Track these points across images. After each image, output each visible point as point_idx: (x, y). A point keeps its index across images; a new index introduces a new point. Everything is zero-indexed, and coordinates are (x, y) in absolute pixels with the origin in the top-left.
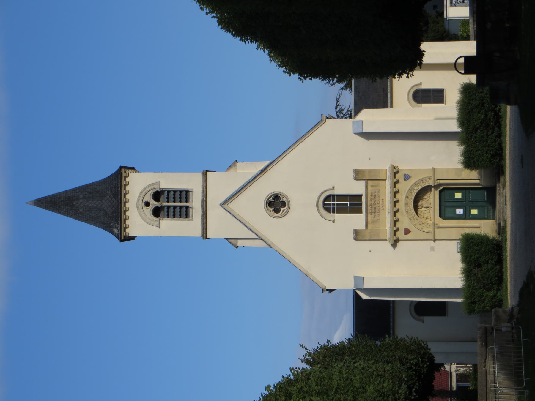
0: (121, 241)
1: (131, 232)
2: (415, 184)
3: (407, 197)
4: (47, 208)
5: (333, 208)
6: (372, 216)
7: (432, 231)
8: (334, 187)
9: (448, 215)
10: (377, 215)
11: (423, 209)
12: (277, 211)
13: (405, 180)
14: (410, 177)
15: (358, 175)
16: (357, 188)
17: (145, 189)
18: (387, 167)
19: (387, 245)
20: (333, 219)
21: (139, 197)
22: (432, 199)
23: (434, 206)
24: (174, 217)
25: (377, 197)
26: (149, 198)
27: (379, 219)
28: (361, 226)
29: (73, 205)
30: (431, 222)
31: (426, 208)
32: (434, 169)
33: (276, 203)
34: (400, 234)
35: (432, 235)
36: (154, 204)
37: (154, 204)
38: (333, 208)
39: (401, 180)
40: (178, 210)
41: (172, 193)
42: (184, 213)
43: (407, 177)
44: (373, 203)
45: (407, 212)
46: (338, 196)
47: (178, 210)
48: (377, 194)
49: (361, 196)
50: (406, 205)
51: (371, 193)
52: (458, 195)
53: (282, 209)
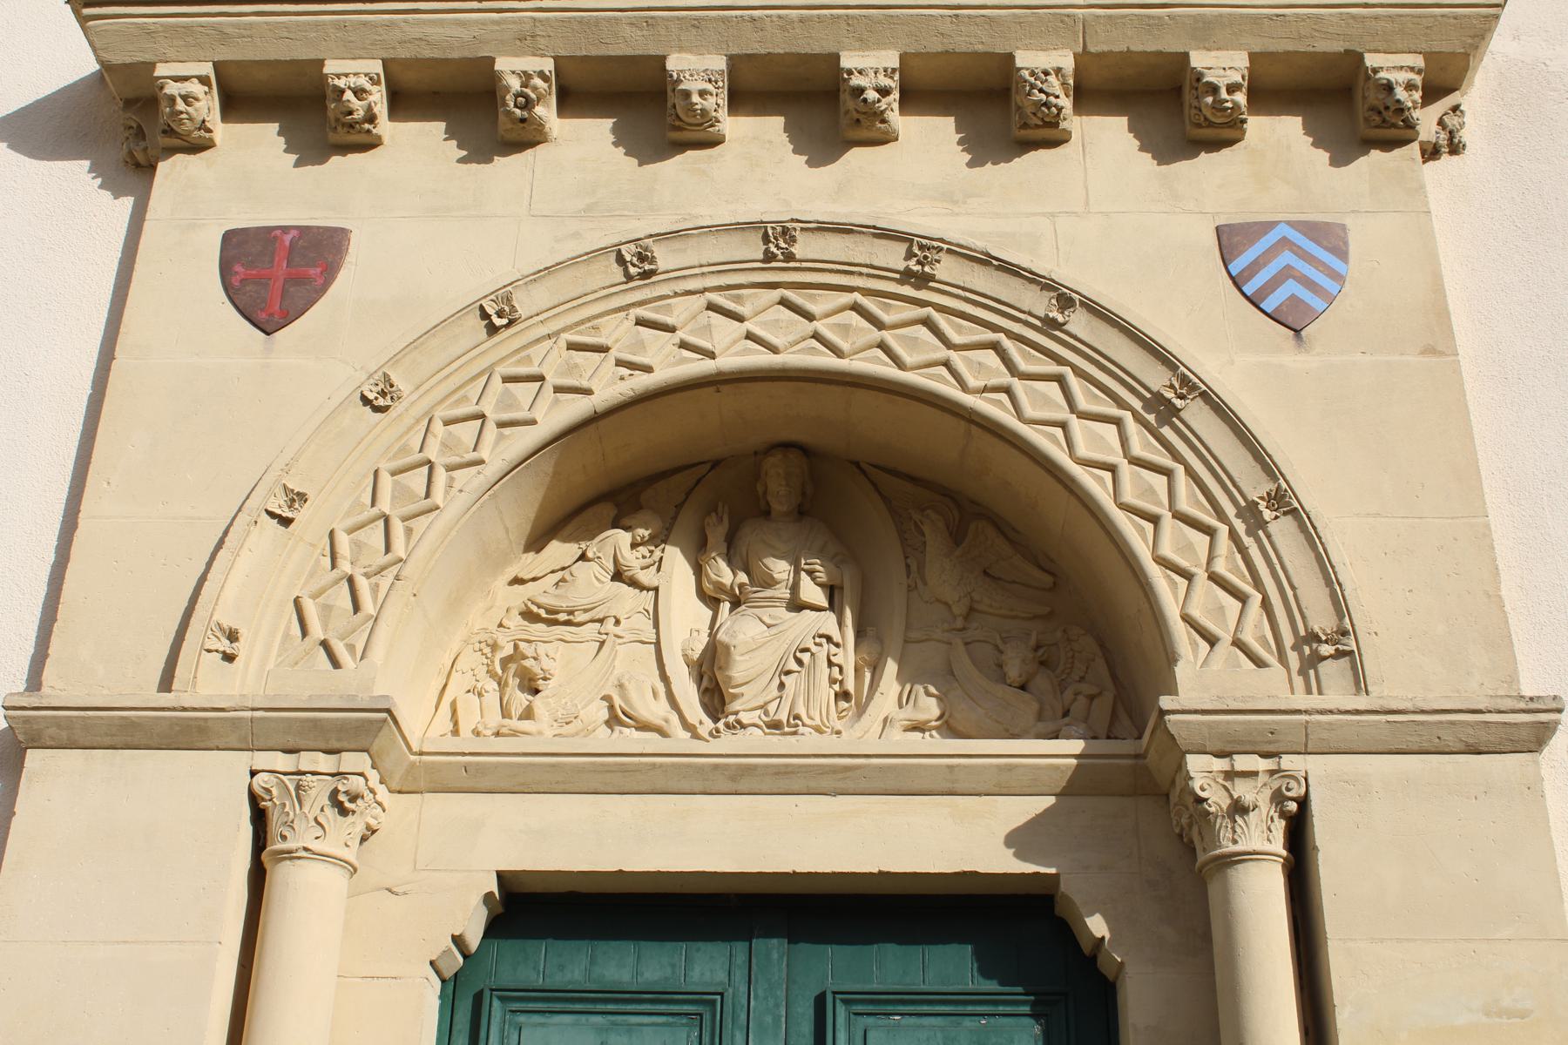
2: (1170, 399)
3: (920, 261)
7: (208, 685)
11: (687, 621)
13: (1229, 240)
23: (739, 779)
31: (712, 677)
34: (248, 174)
35: (130, 684)
43: (1274, 277)
45: (637, 264)
50: (777, 240)
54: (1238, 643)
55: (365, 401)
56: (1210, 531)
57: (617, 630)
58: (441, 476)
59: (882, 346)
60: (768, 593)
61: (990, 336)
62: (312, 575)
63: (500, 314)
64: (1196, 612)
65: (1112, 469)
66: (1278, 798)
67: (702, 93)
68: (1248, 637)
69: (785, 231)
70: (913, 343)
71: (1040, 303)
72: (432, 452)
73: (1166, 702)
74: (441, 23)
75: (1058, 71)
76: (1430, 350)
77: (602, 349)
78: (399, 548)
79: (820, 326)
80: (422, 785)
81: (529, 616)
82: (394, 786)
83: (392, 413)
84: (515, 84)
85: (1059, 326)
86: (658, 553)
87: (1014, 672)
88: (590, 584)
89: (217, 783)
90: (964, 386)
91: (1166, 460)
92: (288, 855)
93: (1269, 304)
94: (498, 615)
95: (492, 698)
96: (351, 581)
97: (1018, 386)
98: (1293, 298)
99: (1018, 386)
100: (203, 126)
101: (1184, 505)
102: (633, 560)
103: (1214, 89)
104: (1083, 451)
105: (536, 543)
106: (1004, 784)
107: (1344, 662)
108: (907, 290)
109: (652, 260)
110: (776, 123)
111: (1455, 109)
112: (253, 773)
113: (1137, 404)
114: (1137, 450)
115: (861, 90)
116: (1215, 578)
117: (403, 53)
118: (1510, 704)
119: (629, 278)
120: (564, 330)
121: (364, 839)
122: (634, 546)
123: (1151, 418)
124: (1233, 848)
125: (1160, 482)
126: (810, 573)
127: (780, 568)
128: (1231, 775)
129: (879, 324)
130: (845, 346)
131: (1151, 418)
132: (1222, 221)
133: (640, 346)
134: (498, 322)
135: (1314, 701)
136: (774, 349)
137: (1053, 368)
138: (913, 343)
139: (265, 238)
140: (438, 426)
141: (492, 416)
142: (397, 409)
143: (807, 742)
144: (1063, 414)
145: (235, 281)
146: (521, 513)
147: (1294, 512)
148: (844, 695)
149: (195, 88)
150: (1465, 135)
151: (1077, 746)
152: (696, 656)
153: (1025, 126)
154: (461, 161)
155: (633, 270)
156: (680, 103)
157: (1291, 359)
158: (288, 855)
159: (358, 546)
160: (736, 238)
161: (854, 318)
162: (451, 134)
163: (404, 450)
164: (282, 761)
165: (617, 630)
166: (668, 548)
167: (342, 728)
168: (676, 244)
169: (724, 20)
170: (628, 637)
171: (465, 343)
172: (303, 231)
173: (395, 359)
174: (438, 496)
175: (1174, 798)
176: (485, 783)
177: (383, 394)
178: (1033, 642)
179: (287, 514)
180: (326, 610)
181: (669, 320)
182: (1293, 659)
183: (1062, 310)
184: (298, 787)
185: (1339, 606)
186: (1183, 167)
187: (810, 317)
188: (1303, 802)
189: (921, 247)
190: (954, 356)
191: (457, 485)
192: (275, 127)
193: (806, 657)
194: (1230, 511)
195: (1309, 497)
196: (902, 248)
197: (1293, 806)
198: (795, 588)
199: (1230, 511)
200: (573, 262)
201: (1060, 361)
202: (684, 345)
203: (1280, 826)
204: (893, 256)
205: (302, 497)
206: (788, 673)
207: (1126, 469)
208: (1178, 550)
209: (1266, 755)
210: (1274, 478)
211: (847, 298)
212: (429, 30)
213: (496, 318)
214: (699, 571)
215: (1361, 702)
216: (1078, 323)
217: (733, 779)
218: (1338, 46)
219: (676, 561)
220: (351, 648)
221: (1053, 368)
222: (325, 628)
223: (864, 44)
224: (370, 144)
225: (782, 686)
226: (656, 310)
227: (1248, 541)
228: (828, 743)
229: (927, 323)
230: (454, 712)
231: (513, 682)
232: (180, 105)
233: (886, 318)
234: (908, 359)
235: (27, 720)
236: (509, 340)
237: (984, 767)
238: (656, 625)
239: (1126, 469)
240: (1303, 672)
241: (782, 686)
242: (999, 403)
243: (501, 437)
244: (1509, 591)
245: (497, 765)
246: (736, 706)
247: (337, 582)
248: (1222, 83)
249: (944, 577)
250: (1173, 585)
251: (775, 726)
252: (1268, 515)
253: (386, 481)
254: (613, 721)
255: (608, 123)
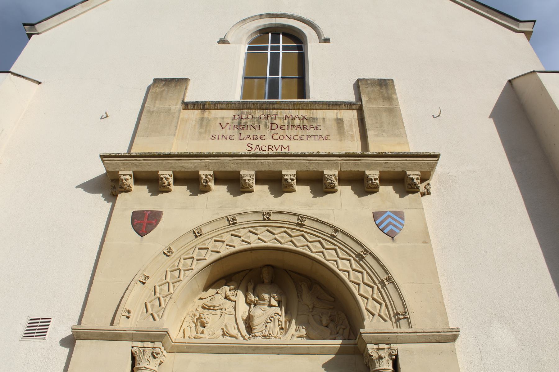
2: (362, 255)
3: (301, 221)
6: (230, 121)
7: (122, 324)
8: (327, 40)
10: (228, 132)
11: (243, 309)
13: (376, 215)
14: (391, 235)
20: (229, 39)
25: (300, 132)
27: (214, 137)
31: (249, 323)
32: (452, 337)
34: (139, 198)
35: (103, 324)
39: (373, 202)
43: (387, 224)
44: (277, 121)
45: (232, 221)
48: (312, 132)
50: (266, 215)
51: (314, 119)
54: (379, 315)
55: (165, 253)
56: (372, 287)
57: (225, 312)
58: (182, 272)
59: (292, 241)
60: (263, 302)
61: (318, 239)
62: (149, 297)
63: (198, 233)
64: (369, 308)
65: (348, 272)
66: (390, 355)
67: (249, 180)
68: (382, 314)
69: (268, 213)
70: (299, 241)
71: (330, 231)
72: (180, 267)
73: (362, 331)
74: (187, 163)
75: (334, 175)
76: (425, 242)
77: (223, 242)
78: (171, 290)
79: (276, 236)
80: (175, 351)
81: (203, 308)
82: (168, 351)
83: (171, 257)
84: (204, 177)
85: (335, 237)
86: (236, 292)
87: (324, 322)
88: (219, 300)
89: (124, 349)
90: (312, 252)
91: (361, 270)
92: (140, 369)
93: (386, 231)
94: (196, 307)
95: (194, 328)
96: (159, 298)
97: (325, 251)
98: (392, 230)
99: (325, 251)
100: (129, 186)
101: (366, 281)
102: (230, 294)
103: (371, 180)
104: (341, 267)
105: (206, 289)
106: (322, 351)
107: (406, 320)
108: (298, 228)
109: (236, 220)
110: (266, 187)
111: (428, 184)
112: (132, 347)
113: (354, 256)
114: (354, 267)
115: (287, 179)
116: (374, 299)
117: (177, 170)
118: (447, 330)
119: (230, 224)
120: (214, 237)
121: (160, 365)
122: (230, 290)
123: (357, 259)
124: (379, 368)
125: (360, 275)
126: (274, 297)
127: (266, 296)
128: (378, 349)
129: (291, 236)
130: (282, 241)
131: (357, 259)
132: (374, 211)
133: (232, 241)
134: (198, 234)
135: (399, 330)
136: (265, 242)
137: (333, 247)
138: (299, 241)
139: (143, 213)
140: (182, 260)
141: (195, 258)
142: (172, 256)
143: (272, 341)
144: (336, 258)
145: (135, 224)
146: (202, 282)
147: (393, 282)
148: (282, 329)
149: (128, 177)
150: (431, 190)
151: (340, 342)
152: (245, 318)
153: (326, 188)
154: (190, 195)
155: (231, 222)
156: (243, 182)
157: (391, 244)
158: (140, 369)
159: (161, 290)
160: (256, 215)
161: (285, 234)
162: (188, 189)
163: (174, 266)
164: (140, 344)
165: (225, 312)
166: (239, 291)
167: (155, 336)
168: (242, 216)
169: (254, 162)
170: (228, 313)
171: (189, 240)
172: (152, 211)
173: (172, 243)
174: (181, 278)
175: (364, 355)
176: (191, 351)
177: (169, 252)
178: (329, 315)
179: (144, 281)
180: (153, 306)
181: (240, 235)
182: (393, 319)
183: (335, 233)
184: (144, 351)
185: (404, 306)
186: (364, 198)
187: (274, 234)
188: (397, 356)
189: (301, 217)
190: (309, 244)
191: (186, 275)
192: (146, 186)
193: (272, 319)
194: (377, 282)
195: (397, 278)
196: (297, 217)
197: (394, 357)
198: (270, 301)
199: (377, 282)
200: (216, 220)
201: (335, 245)
202: (243, 241)
203: (391, 362)
204: (294, 219)
205: (148, 277)
206: (268, 323)
207: (351, 272)
208: (365, 292)
209: (387, 344)
210: (388, 274)
211: (283, 230)
212: (184, 164)
213: (197, 234)
214: (246, 297)
215: (410, 330)
216: (340, 236)
217: (253, 350)
218: (400, 170)
219: (240, 294)
220: (158, 316)
221: (333, 247)
222: (152, 310)
223: (288, 169)
224: (169, 191)
225: (266, 326)
226: (236, 232)
227: (382, 290)
228: (278, 341)
229: (303, 236)
230: (184, 332)
231: (199, 324)
232: (124, 181)
233: (293, 234)
234: (298, 245)
235: (77, 332)
236: (200, 239)
237: (317, 347)
238: (235, 310)
239: (351, 272)
240: (396, 323)
241: (266, 326)
242: (320, 256)
243: (197, 263)
244: (445, 301)
245: (194, 346)
246: (255, 331)
247: (156, 298)
248: (373, 178)
249: (307, 299)
250: (363, 301)
251: (264, 336)
252: (386, 283)
253: (169, 273)
254: (224, 335)
255: (226, 187)
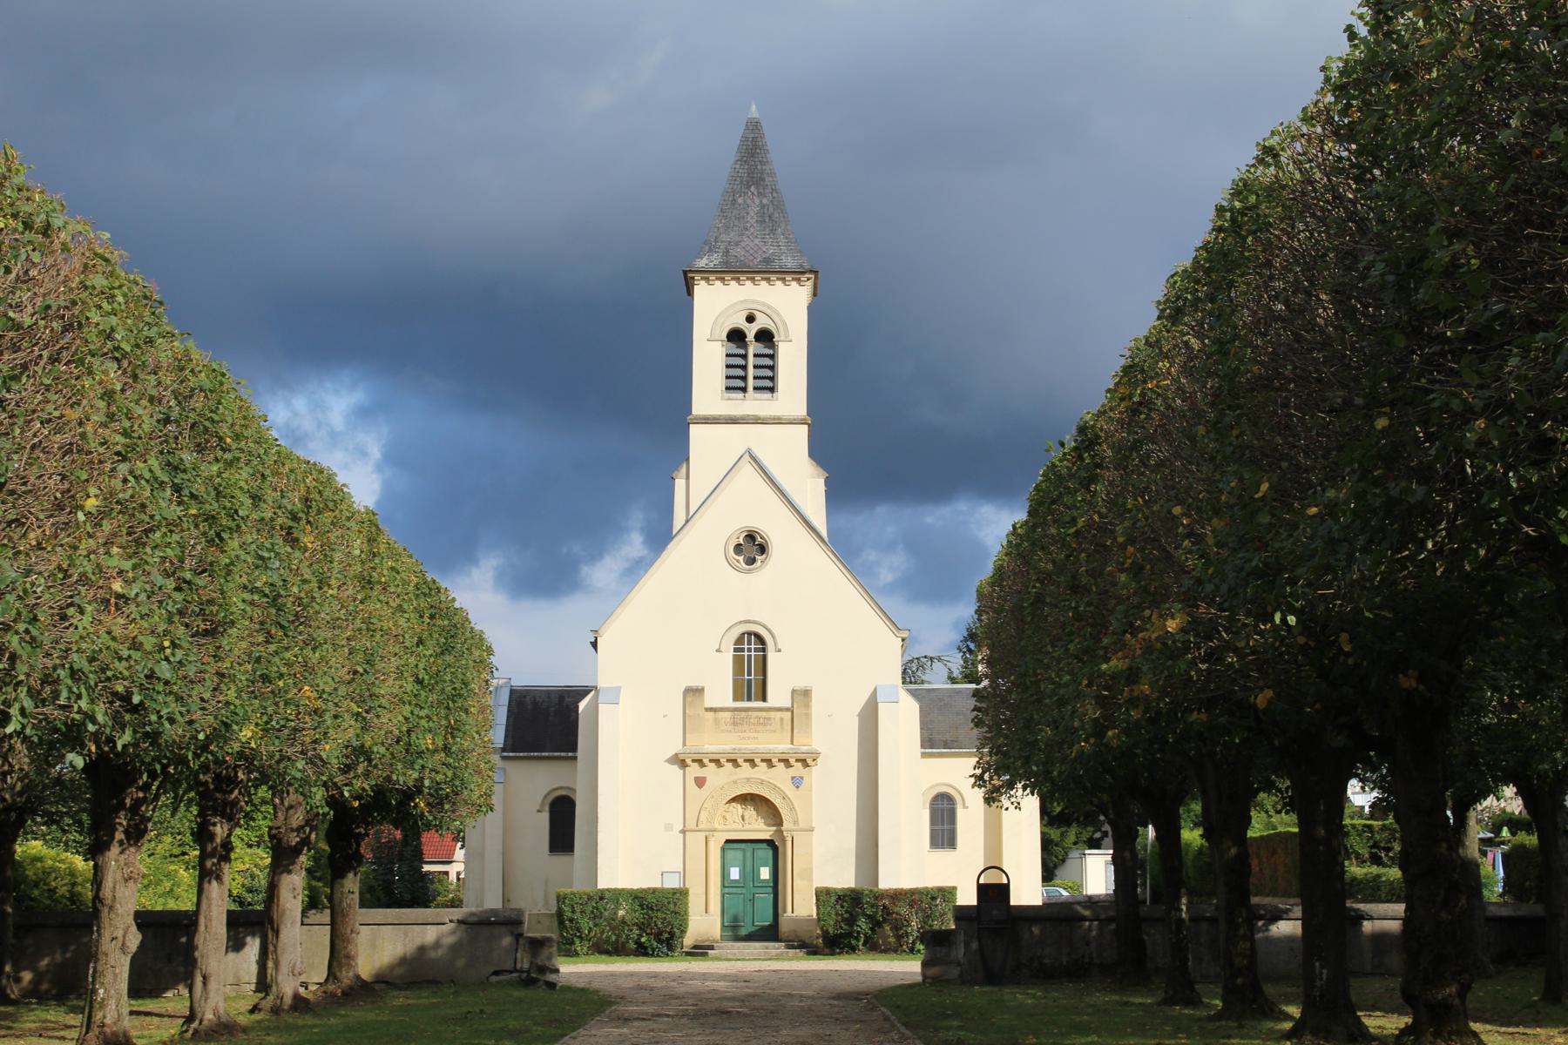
0: (685, 273)
1: (701, 290)
4: (745, 139)
5: (742, 650)
7: (701, 827)
9: (731, 855)
12: (738, 549)
15: (802, 695)
16: (778, 693)
17: (778, 314)
18: (815, 746)
19: (676, 747)
21: (764, 304)
22: (759, 828)
24: (728, 366)
26: (761, 322)
28: (710, 700)
29: (749, 187)
30: (717, 826)
33: (752, 547)
34: (694, 770)
36: (751, 331)
37: (751, 331)
38: (742, 650)
40: (740, 372)
41: (770, 363)
42: (736, 383)
43: (797, 782)
46: (765, 658)
47: (740, 372)
49: (764, 699)
52: (765, 873)
53: (741, 558)
249: (765, 808)
